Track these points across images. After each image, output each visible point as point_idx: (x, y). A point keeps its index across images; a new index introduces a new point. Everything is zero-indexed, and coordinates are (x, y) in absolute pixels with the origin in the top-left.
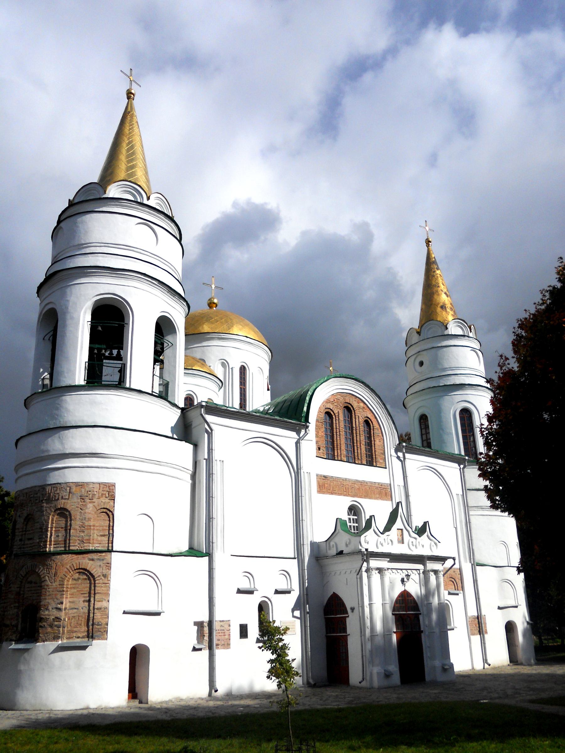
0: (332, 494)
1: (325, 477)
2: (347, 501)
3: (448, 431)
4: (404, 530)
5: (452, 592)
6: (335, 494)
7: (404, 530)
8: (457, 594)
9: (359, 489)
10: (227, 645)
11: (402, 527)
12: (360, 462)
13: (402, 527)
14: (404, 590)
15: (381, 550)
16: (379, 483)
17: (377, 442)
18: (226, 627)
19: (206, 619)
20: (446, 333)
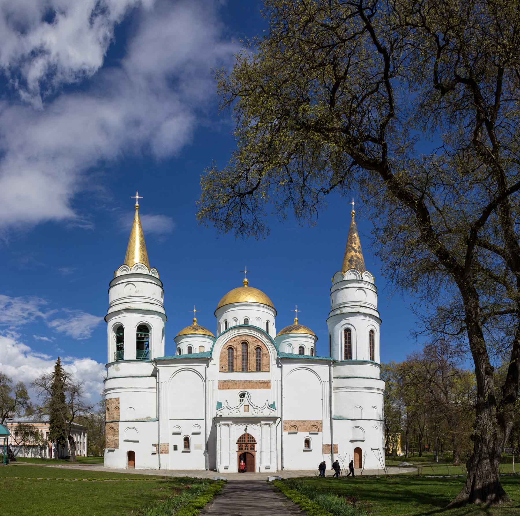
0: (229, 389)
1: (225, 381)
2: (239, 391)
3: (337, 343)
4: (250, 405)
5: (312, 432)
6: (231, 389)
7: (250, 405)
8: (317, 434)
9: (247, 385)
10: (167, 452)
11: (249, 404)
12: (250, 371)
13: (248, 404)
14: (244, 432)
15: (231, 415)
16: (262, 380)
17: (264, 359)
18: (166, 446)
19: (157, 443)
20: (344, 280)
